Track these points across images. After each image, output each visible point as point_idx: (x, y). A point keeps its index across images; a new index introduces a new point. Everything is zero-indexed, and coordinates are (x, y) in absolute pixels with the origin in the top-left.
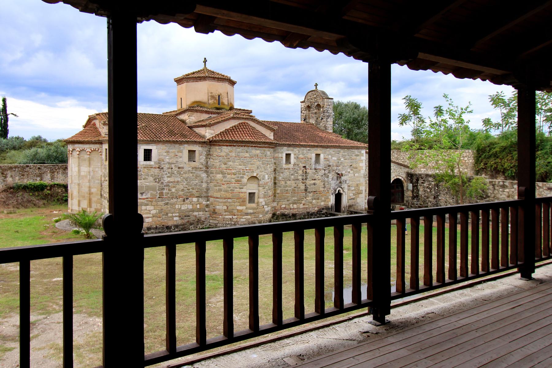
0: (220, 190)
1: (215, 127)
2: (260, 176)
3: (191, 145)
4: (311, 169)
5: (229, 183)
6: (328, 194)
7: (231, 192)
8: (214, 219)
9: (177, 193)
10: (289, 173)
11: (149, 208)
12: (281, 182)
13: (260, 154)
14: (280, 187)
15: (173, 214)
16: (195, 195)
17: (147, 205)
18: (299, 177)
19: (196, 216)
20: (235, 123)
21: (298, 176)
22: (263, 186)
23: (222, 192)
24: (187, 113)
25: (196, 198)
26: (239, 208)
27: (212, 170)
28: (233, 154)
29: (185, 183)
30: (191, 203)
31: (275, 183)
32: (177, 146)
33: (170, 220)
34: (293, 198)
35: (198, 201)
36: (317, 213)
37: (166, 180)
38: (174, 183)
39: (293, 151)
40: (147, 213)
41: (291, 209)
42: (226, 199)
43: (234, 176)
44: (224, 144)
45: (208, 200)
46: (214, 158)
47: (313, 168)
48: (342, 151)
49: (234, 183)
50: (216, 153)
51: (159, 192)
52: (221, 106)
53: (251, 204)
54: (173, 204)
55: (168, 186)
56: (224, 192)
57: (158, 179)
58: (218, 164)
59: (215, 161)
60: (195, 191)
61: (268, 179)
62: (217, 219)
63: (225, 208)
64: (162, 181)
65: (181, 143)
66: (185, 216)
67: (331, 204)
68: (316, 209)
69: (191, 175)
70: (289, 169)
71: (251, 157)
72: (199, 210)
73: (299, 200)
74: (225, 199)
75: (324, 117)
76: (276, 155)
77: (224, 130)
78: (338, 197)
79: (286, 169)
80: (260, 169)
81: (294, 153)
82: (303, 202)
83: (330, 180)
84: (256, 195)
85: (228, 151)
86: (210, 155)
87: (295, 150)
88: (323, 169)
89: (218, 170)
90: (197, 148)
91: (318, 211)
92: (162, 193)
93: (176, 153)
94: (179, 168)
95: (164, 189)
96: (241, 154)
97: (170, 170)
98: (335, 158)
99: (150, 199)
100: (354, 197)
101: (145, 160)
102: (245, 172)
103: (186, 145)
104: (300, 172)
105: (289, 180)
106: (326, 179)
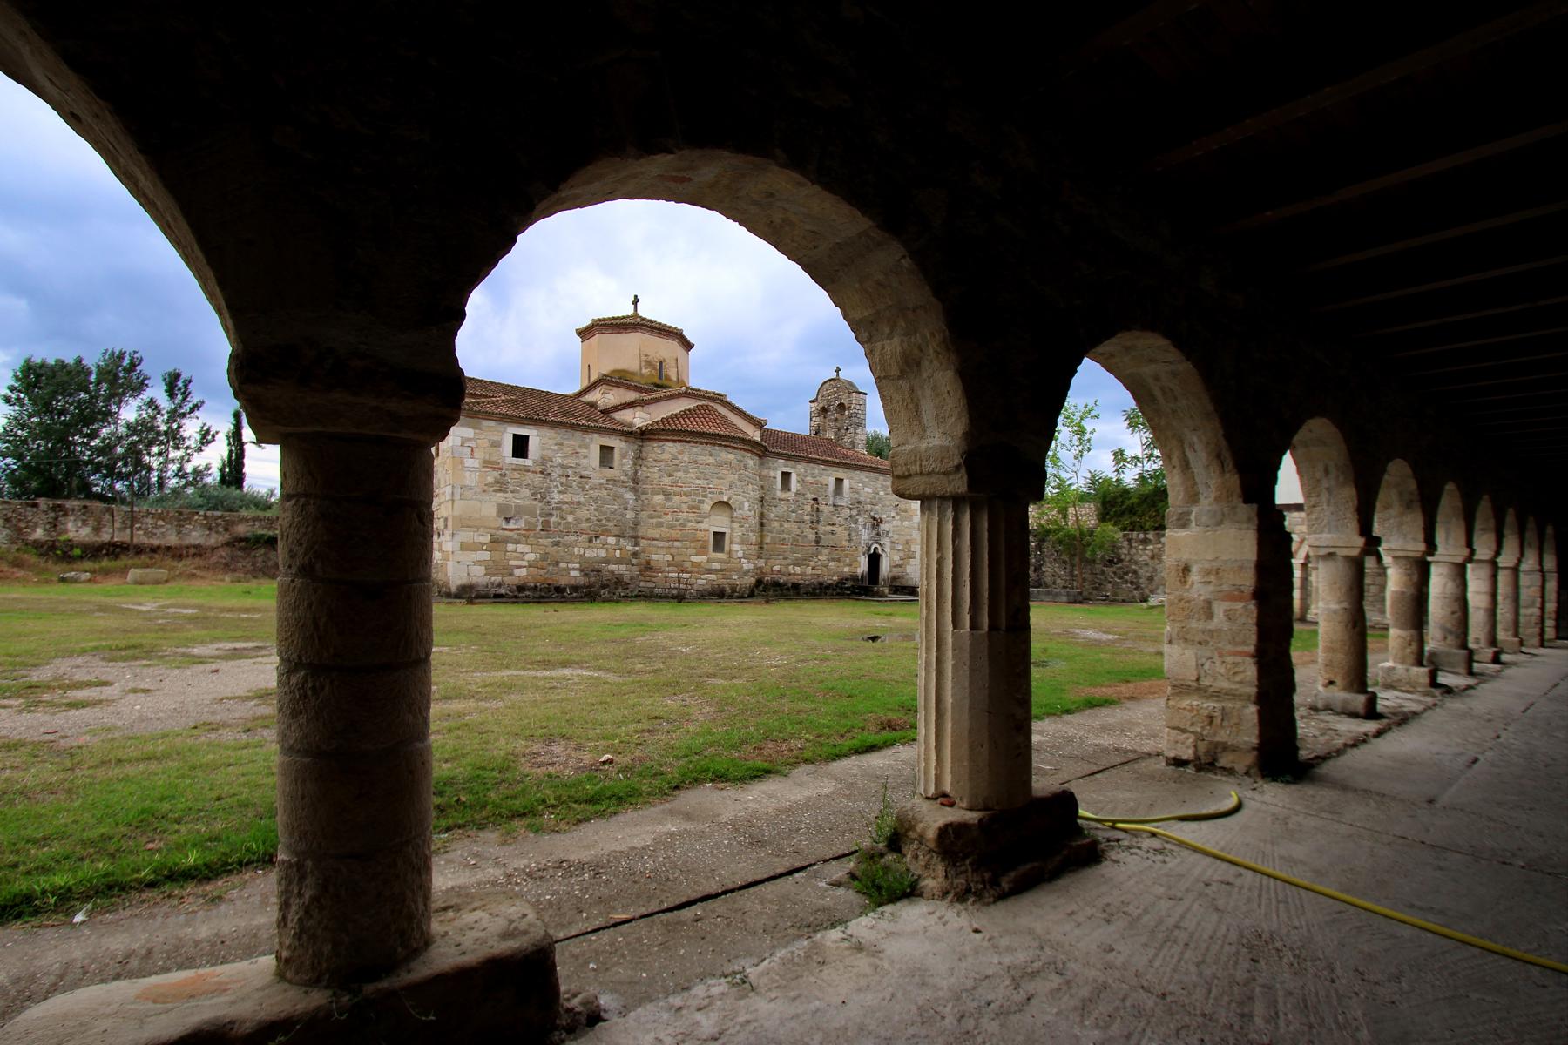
0: (660, 525)
1: (652, 407)
6: (855, 554)
8: (648, 579)
11: (520, 548)
14: (771, 532)
15: (570, 565)
17: (517, 542)
19: (612, 572)
21: (803, 515)
22: (740, 522)
23: (664, 529)
30: (604, 546)
31: (762, 525)
32: (578, 434)
35: (618, 543)
37: (557, 497)
45: (636, 544)
46: (650, 464)
48: (881, 478)
51: (541, 519)
52: (664, 382)
55: (560, 509)
57: (540, 495)
58: (657, 475)
60: (610, 524)
61: (750, 510)
63: (669, 557)
65: (587, 430)
66: (593, 571)
69: (605, 492)
71: (719, 465)
72: (619, 561)
76: (765, 472)
81: (797, 471)
82: (812, 564)
83: (860, 528)
84: (727, 537)
87: (799, 466)
90: (616, 443)
94: (581, 477)
95: (551, 514)
96: (700, 458)
98: (870, 490)
100: (901, 562)
103: (596, 435)
104: (808, 508)
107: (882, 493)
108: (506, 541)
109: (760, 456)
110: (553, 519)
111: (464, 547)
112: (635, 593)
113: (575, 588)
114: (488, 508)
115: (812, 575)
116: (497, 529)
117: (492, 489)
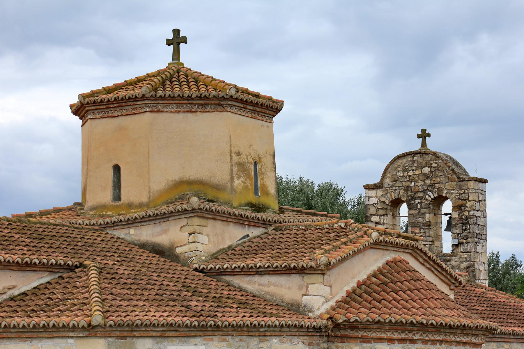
1: (333, 275)
3: (286, 339)
24: (184, 222)
44: (383, 335)
75: (467, 238)
77: (353, 284)
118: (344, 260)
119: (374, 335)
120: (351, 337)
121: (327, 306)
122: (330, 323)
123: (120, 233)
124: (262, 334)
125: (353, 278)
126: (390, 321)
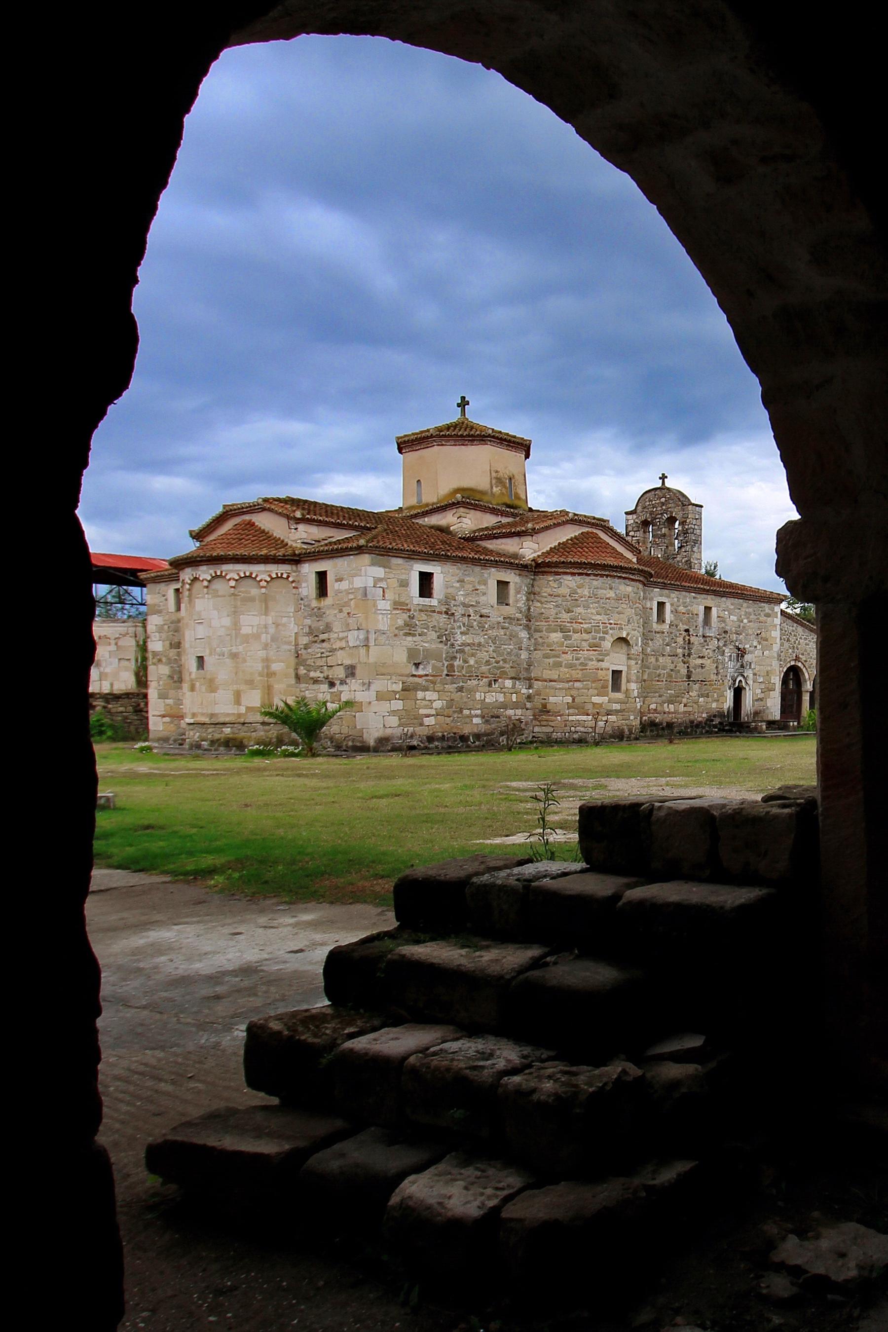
0: (558, 665)
2: (632, 638)
3: (501, 570)
4: (697, 636)
5: (577, 650)
7: (580, 667)
8: (544, 723)
9: (478, 668)
10: (664, 640)
11: (430, 695)
12: (649, 657)
13: (632, 595)
14: (649, 668)
16: (508, 675)
17: (426, 689)
18: (678, 649)
19: (510, 718)
20: (575, 531)
22: (636, 659)
23: (562, 669)
25: (511, 681)
26: (596, 699)
27: (538, 624)
28: (586, 593)
29: (491, 649)
30: (502, 690)
33: (466, 723)
34: (669, 691)
35: (514, 687)
36: (706, 724)
37: (460, 639)
38: (474, 648)
39: (668, 597)
40: (426, 707)
41: (664, 713)
42: (571, 681)
43: (586, 635)
44: (568, 571)
45: (530, 687)
46: (543, 600)
47: (701, 634)
48: (745, 605)
49: (587, 650)
50: (549, 590)
51: (446, 664)
53: (616, 694)
54: (471, 691)
56: (566, 667)
57: (445, 637)
58: (553, 612)
59: (545, 606)
60: (508, 666)
62: (550, 723)
64: (452, 640)
66: (492, 717)
67: (728, 706)
68: (704, 715)
69: (502, 632)
70: (663, 633)
71: (618, 599)
72: (516, 706)
73: (678, 697)
74: (568, 682)
78: (738, 693)
79: (658, 633)
80: (633, 624)
81: (670, 599)
82: (684, 700)
83: (727, 659)
84: (624, 674)
85: (575, 584)
86: (534, 594)
87: (673, 595)
88: (715, 637)
89: (553, 624)
90: (511, 577)
91: (707, 720)
92: (452, 666)
93: (476, 584)
95: (455, 658)
96: (601, 592)
97: (466, 618)
99: (431, 678)
100: (762, 695)
101: (421, 595)
102: (607, 627)
103: (493, 570)
104: (680, 640)
105: (663, 655)
106: (720, 657)
107: (745, 621)
108: (416, 688)
109: (644, 585)
110: (456, 663)
111: (380, 697)
112: (530, 739)
113: (477, 736)
114: (400, 656)
115: (685, 712)
116: (407, 676)
117: (402, 633)
118: (547, 528)
119: (562, 570)
120: (548, 572)
121: (535, 555)
122: (533, 563)
123: (420, 521)
124: (483, 564)
125: (556, 540)
126: (571, 561)
